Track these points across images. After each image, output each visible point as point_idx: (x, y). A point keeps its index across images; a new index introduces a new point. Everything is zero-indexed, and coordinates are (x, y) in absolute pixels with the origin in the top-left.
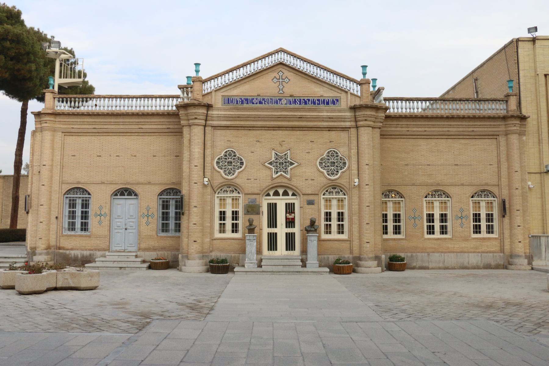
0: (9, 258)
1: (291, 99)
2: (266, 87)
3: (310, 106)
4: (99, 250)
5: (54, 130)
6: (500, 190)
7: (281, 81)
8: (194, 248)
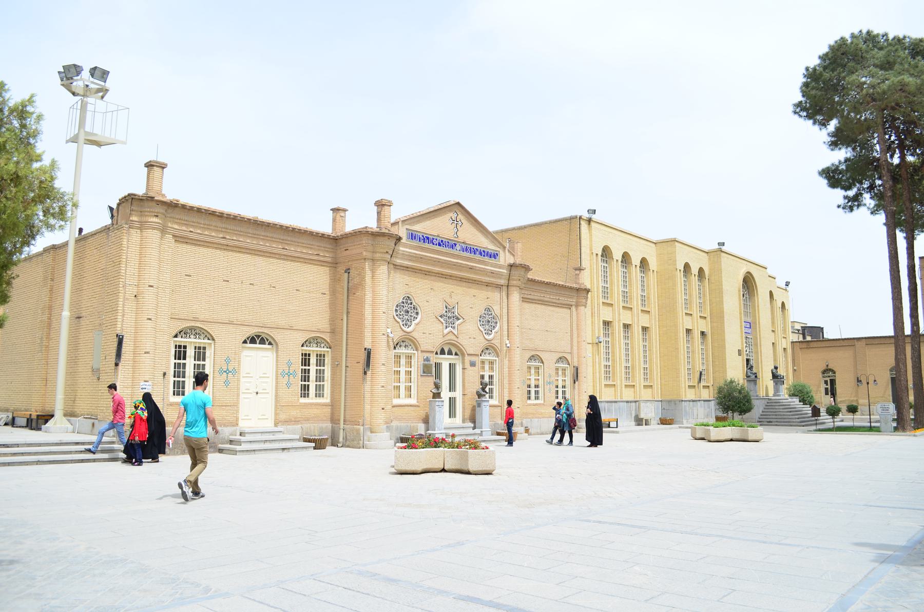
0: (40, 445)
1: (464, 246)
2: (441, 227)
3: (478, 257)
4: (225, 426)
5: (163, 231)
6: (572, 358)
7: (455, 221)
8: (380, 419)
